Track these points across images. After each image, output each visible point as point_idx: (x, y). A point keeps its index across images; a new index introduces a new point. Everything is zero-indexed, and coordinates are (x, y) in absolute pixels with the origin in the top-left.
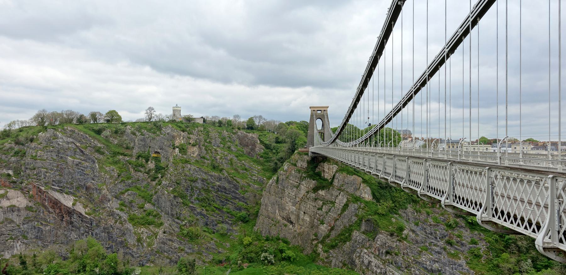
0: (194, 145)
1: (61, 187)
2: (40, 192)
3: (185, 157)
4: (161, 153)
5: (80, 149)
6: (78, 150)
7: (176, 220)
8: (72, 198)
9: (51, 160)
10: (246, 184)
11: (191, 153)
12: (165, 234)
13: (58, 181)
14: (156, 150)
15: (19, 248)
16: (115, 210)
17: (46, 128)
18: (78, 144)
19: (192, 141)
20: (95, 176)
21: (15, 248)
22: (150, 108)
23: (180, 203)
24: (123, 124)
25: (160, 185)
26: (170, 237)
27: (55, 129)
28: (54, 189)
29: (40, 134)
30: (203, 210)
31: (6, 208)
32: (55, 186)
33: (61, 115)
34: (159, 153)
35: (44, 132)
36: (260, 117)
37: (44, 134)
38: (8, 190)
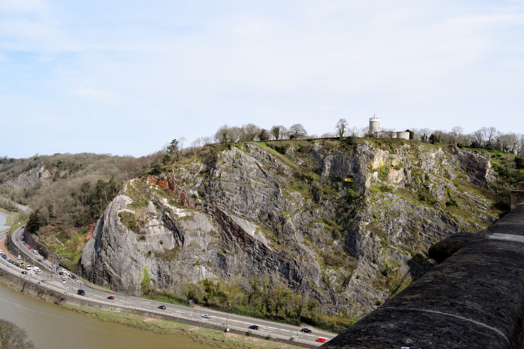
0: (397, 169)
1: (243, 212)
2: (223, 217)
3: (385, 183)
4: (355, 177)
5: (262, 171)
6: (260, 171)
7: (372, 264)
8: (255, 226)
9: (234, 182)
10: (468, 224)
11: (393, 178)
12: (358, 280)
13: (241, 205)
14: (348, 174)
15: (204, 275)
16: (300, 244)
17: (229, 147)
18: (261, 165)
19: (394, 163)
20: (278, 202)
21: (201, 275)
22: (341, 120)
23: (377, 243)
24: (309, 140)
25: (353, 217)
26: (364, 284)
27: (237, 147)
28: (236, 215)
29: (223, 152)
30: (407, 254)
31: (193, 232)
32: (237, 211)
33: (242, 130)
34: (353, 178)
35: (227, 151)
36: (493, 129)
37: (227, 152)
38: (194, 212)
